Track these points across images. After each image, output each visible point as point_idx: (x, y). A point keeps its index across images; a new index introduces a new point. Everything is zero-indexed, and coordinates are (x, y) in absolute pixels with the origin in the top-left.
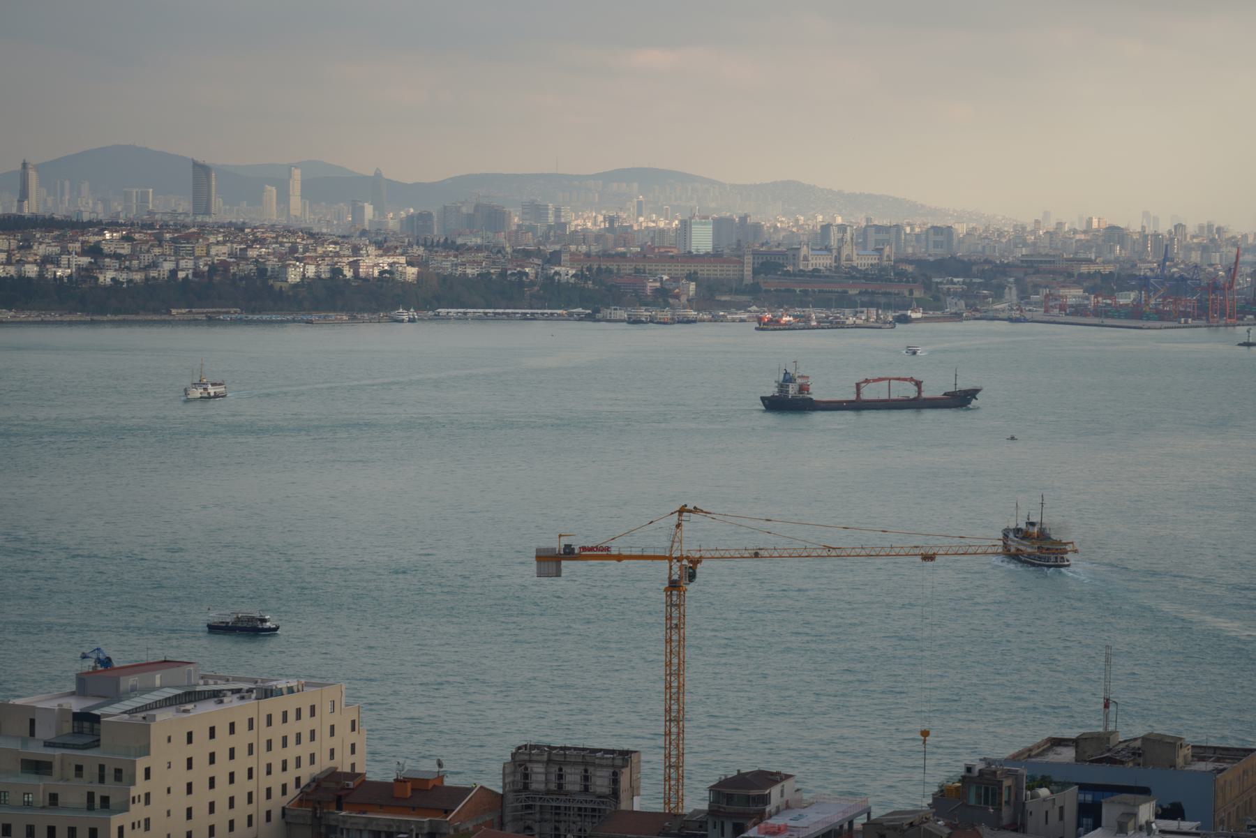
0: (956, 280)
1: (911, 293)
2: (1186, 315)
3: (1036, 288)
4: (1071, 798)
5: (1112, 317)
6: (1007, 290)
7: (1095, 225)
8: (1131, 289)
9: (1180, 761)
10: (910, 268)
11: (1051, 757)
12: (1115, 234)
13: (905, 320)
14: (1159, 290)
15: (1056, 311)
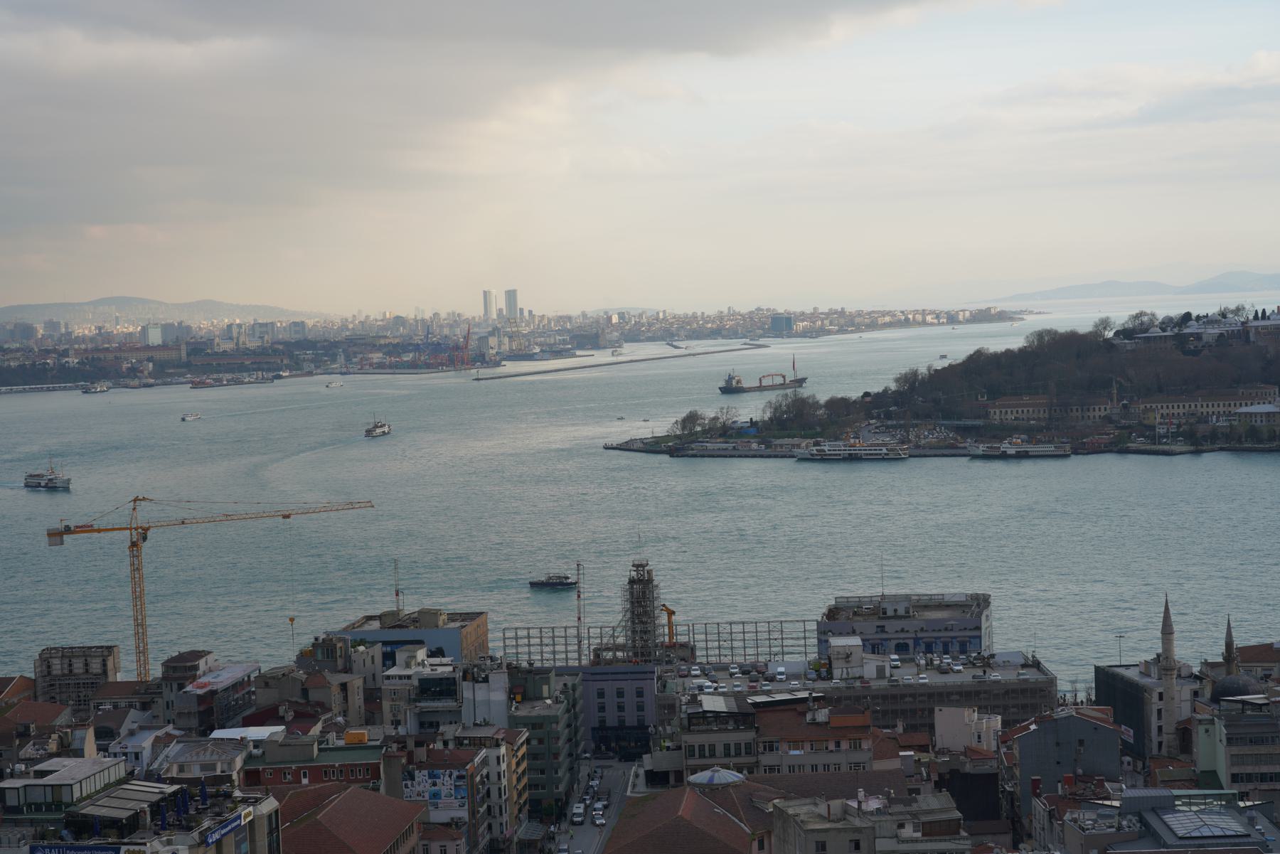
0: (308, 352)
1: (282, 361)
2: (442, 365)
3: (355, 354)
4: (378, 650)
5: (400, 368)
6: (338, 357)
7: (388, 316)
8: (410, 351)
9: (441, 623)
10: (281, 347)
11: (366, 627)
12: (399, 321)
13: (280, 377)
14: (425, 351)
15: (367, 367)
